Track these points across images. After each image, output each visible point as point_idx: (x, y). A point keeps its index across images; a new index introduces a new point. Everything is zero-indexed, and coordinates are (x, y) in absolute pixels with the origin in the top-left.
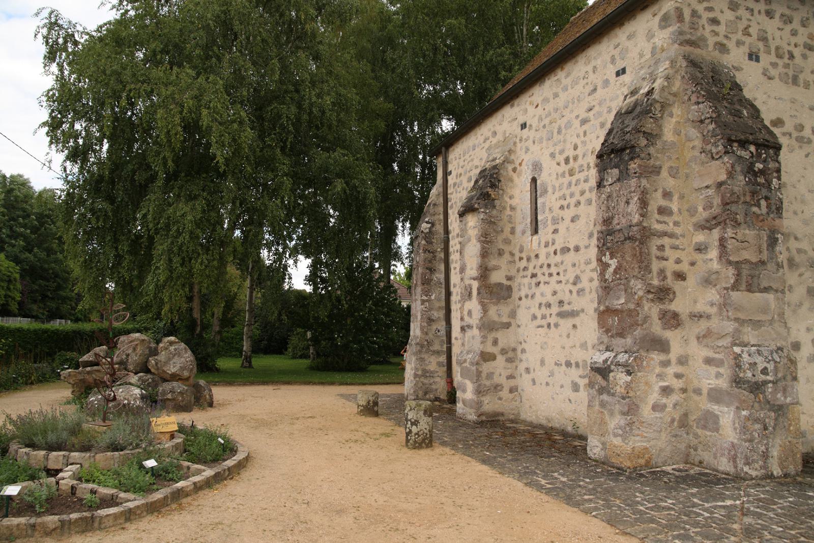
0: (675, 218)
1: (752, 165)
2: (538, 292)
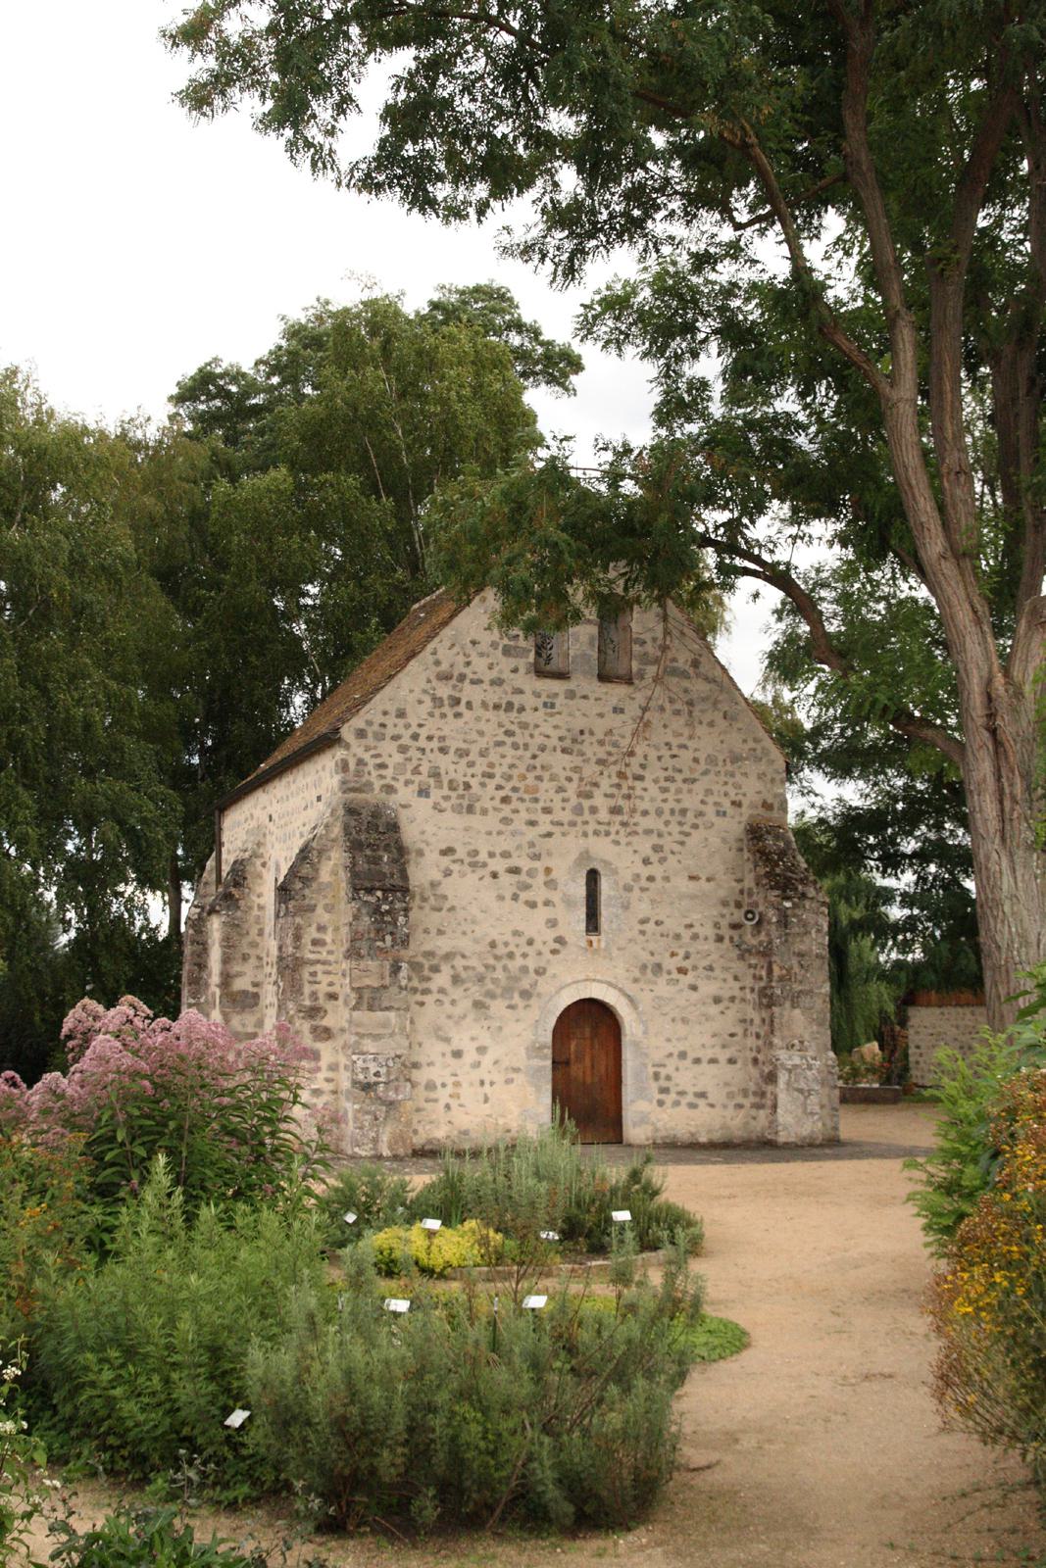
0: (330, 947)
1: (379, 907)
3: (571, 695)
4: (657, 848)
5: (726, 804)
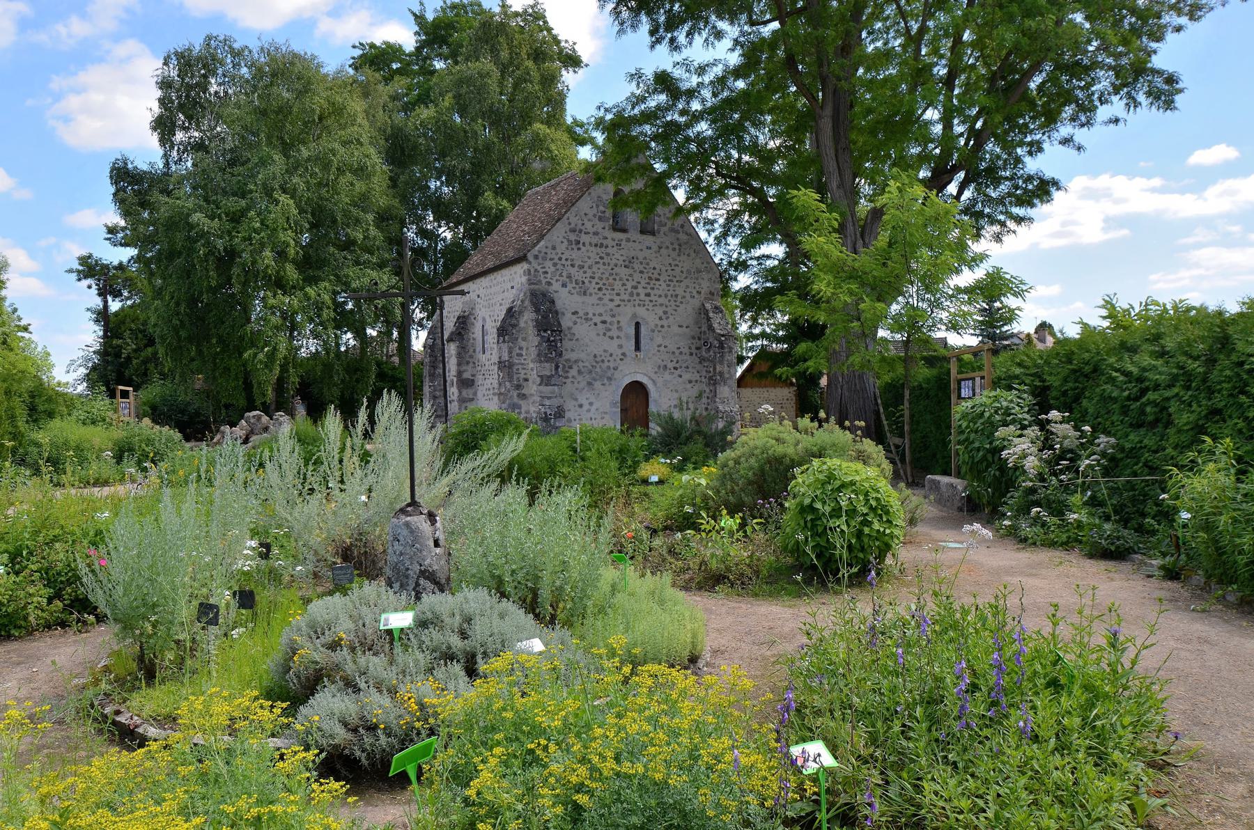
3: (628, 240)
4: (665, 313)
5: (695, 293)
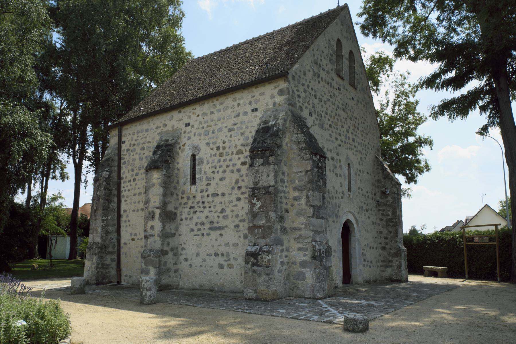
0: (286, 184)
1: (318, 164)
2: (195, 216)
